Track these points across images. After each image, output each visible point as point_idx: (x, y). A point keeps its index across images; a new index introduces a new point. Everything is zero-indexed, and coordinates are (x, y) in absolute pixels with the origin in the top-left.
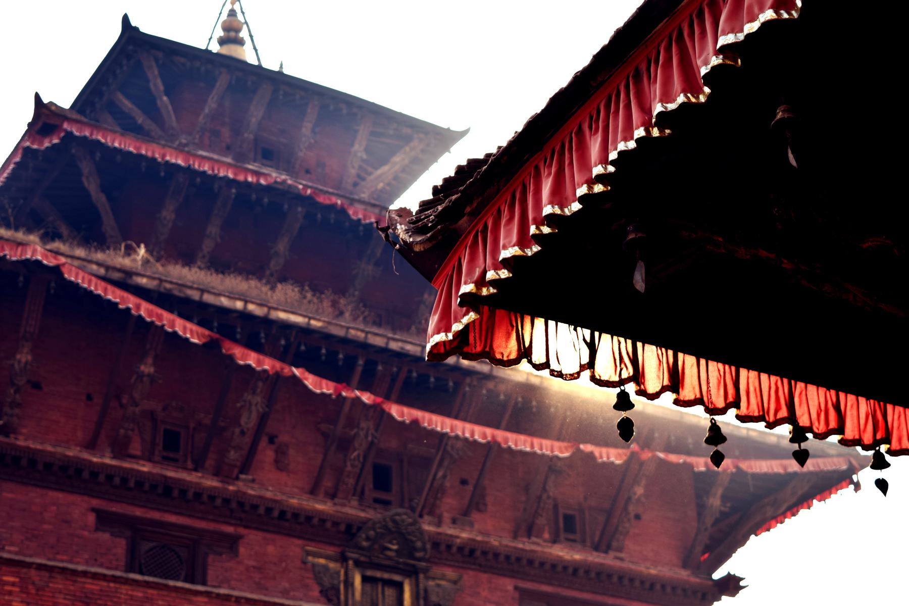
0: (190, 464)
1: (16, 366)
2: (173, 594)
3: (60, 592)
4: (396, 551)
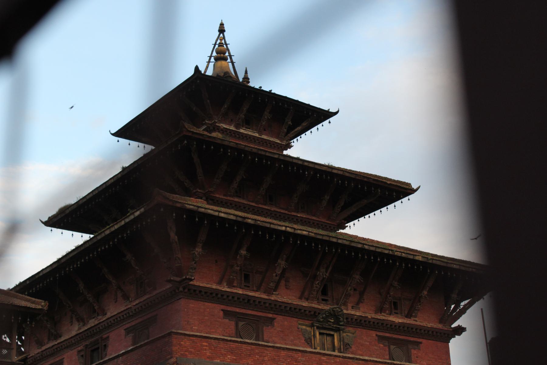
0: (255, 288)
2: (261, 347)
3: (222, 349)
4: (332, 322)
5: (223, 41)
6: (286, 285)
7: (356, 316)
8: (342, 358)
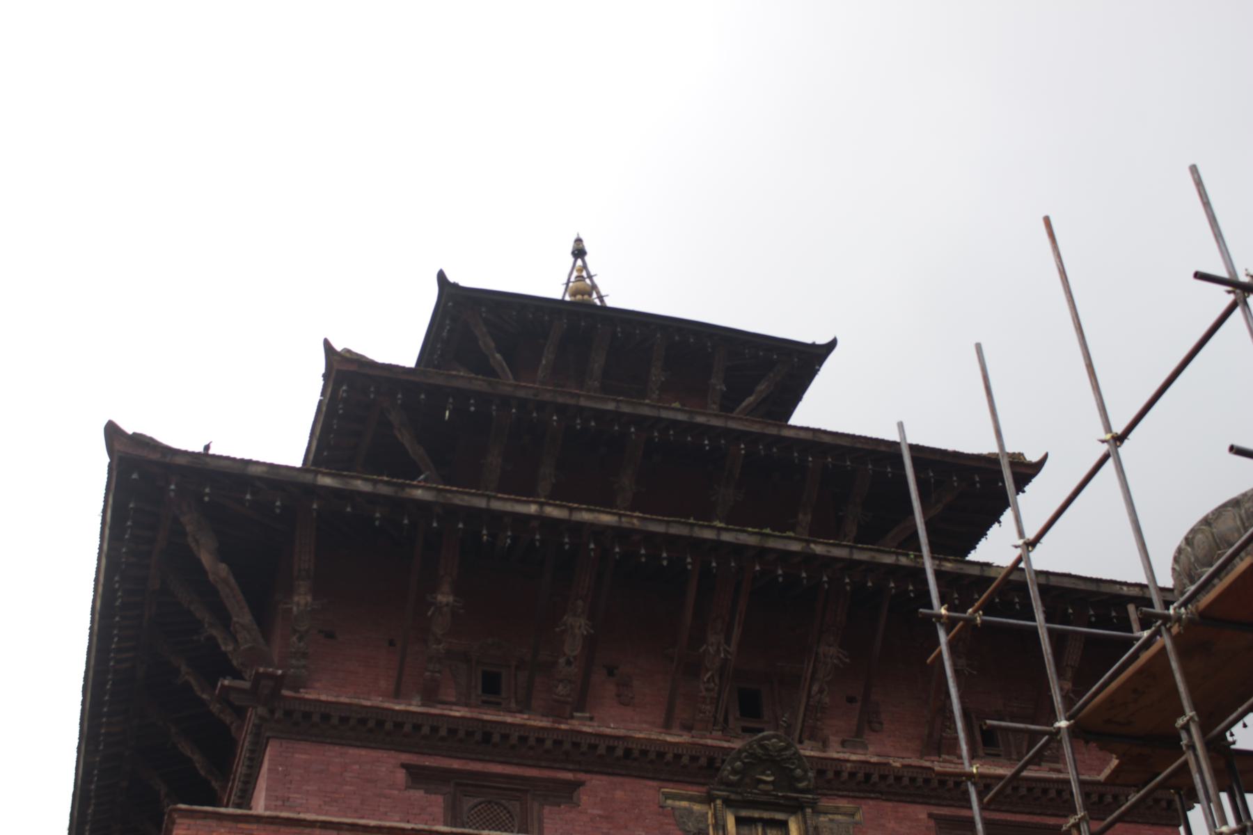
1: (295, 609)
4: (772, 783)
6: (619, 696)
7: (849, 765)
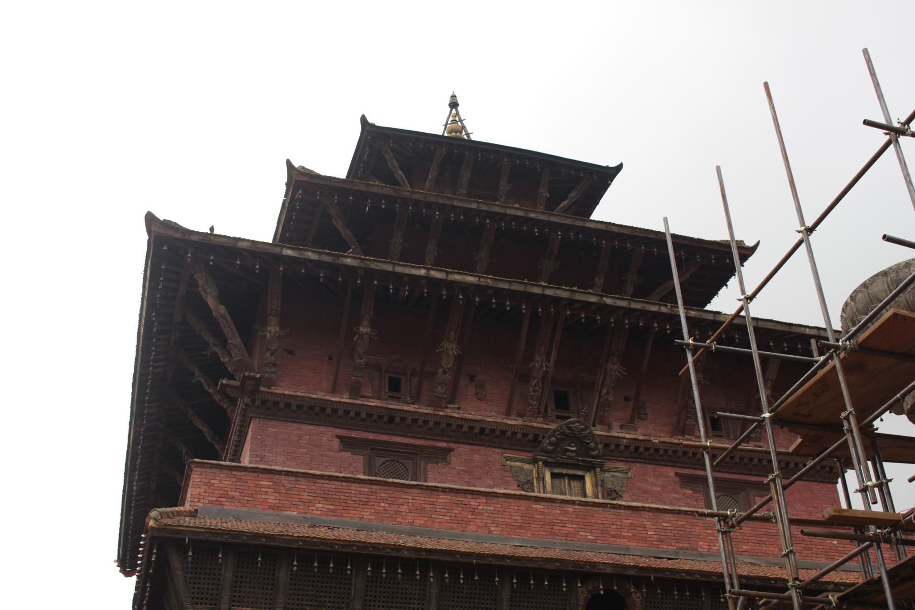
1: (268, 335)
2: (393, 488)
5: (457, 119)
6: (477, 394)
7: (625, 441)
8: (579, 505)
